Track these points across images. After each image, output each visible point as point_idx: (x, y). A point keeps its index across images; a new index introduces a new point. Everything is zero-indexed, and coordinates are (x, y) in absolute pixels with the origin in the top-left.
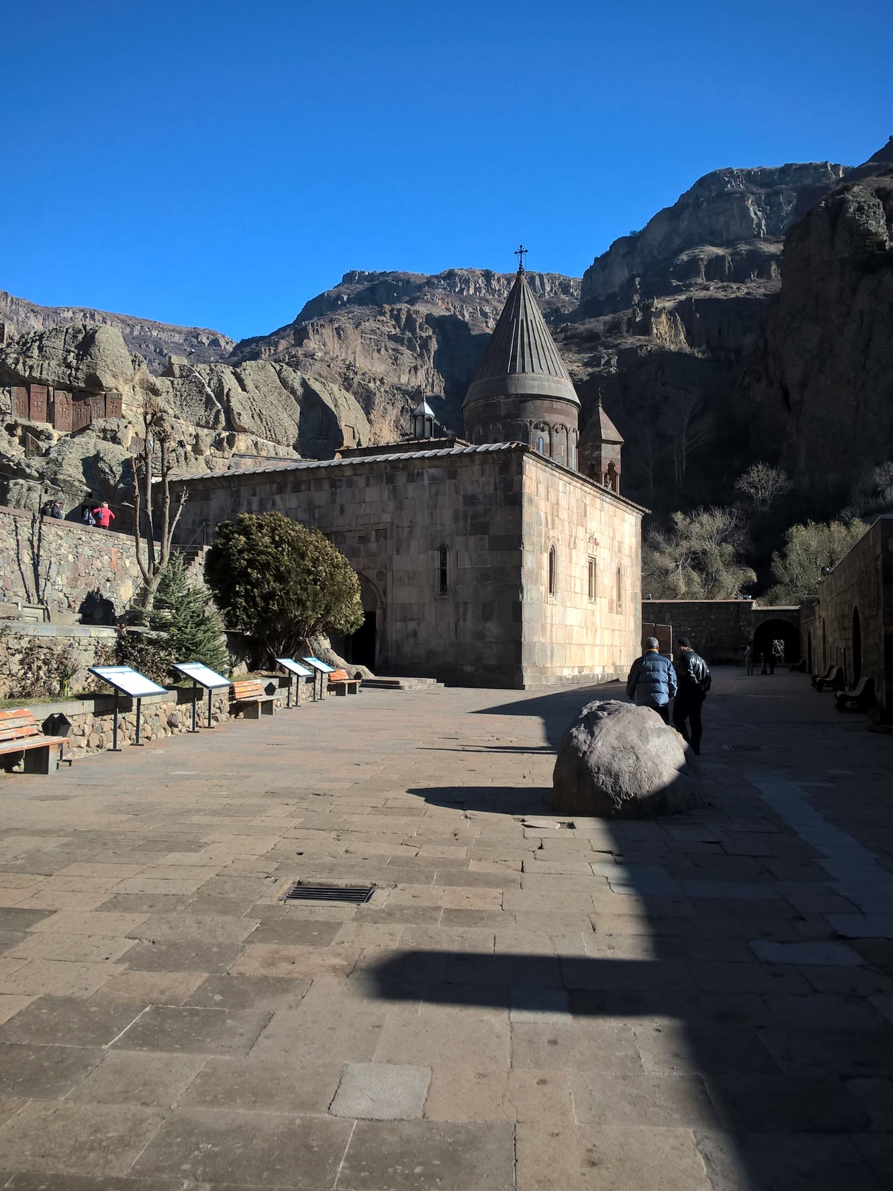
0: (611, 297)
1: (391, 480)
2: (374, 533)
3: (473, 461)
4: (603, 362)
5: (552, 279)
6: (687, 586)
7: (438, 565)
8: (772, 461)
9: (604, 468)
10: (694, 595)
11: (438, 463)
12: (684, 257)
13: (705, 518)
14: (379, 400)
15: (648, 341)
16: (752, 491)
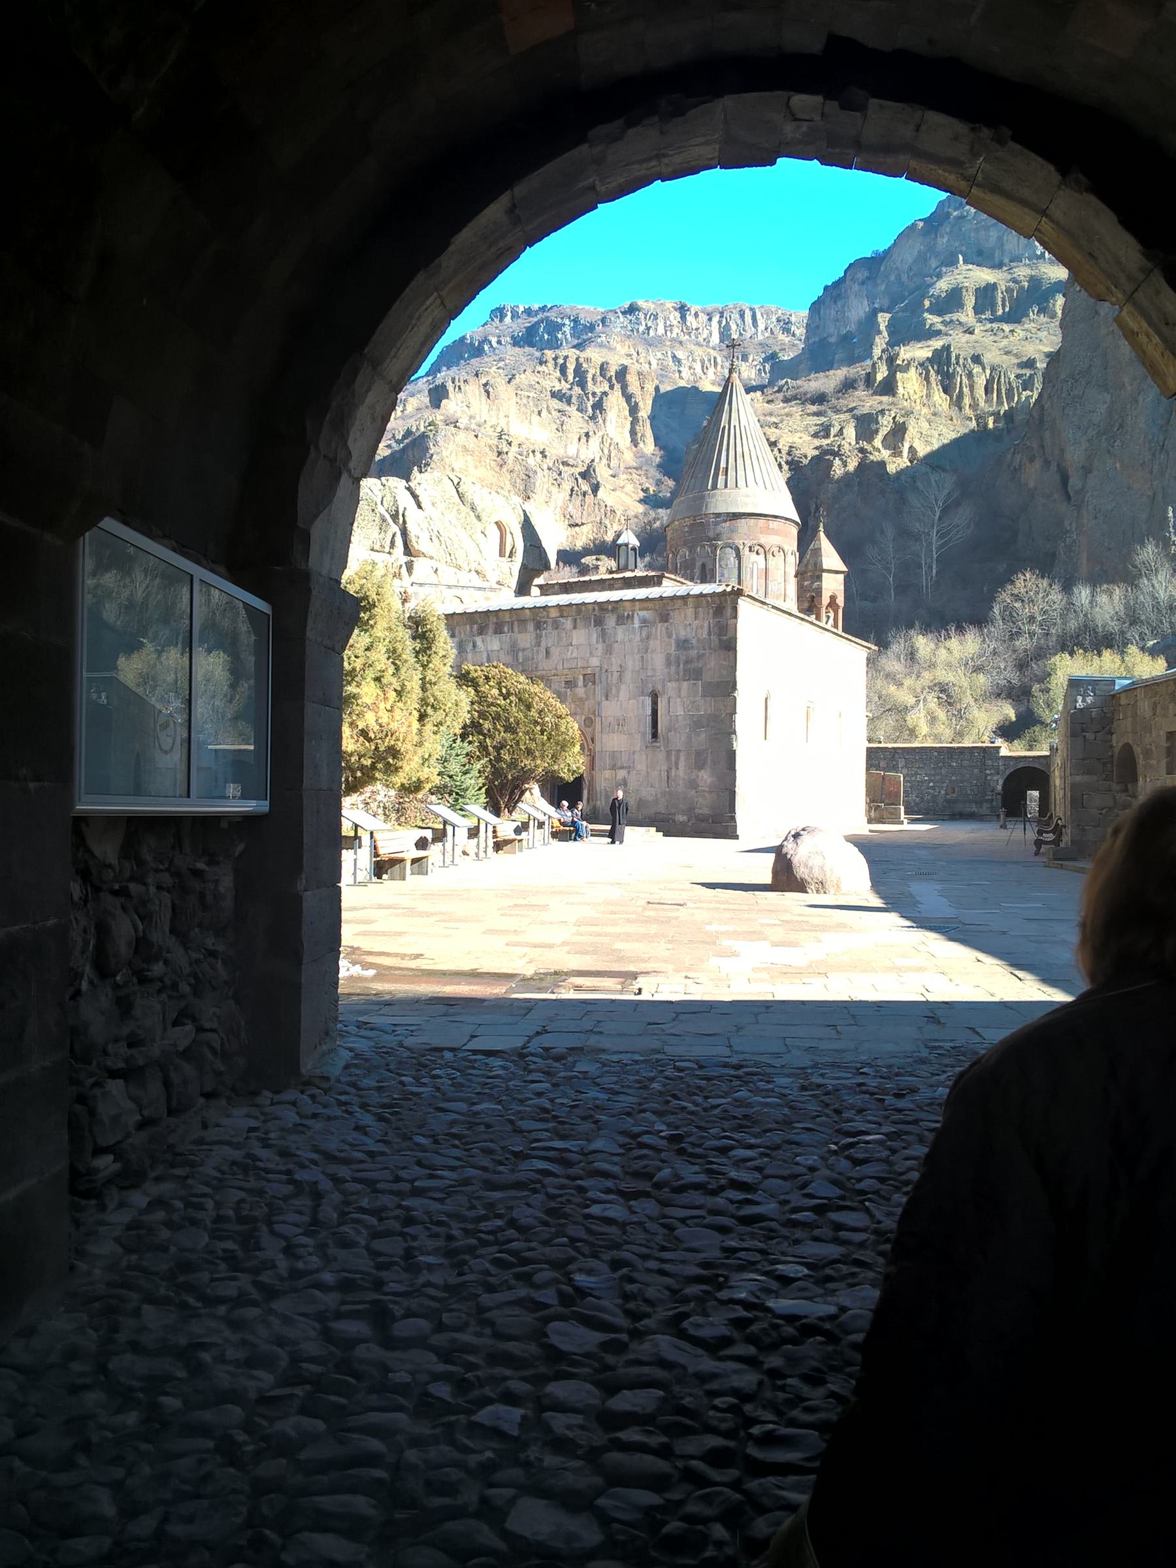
0: (846, 338)
1: (599, 622)
2: (581, 677)
3: (686, 604)
4: (833, 431)
5: (768, 314)
6: (929, 729)
7: (649, 712)
8: (1045, 566)
9: (825, 600)
10: (937, 737)
11: (650, 605)
12: (943, 285)
13: (954, 643)
14: (542, 481)
15: (893, 403)
16: (1018, 605)
